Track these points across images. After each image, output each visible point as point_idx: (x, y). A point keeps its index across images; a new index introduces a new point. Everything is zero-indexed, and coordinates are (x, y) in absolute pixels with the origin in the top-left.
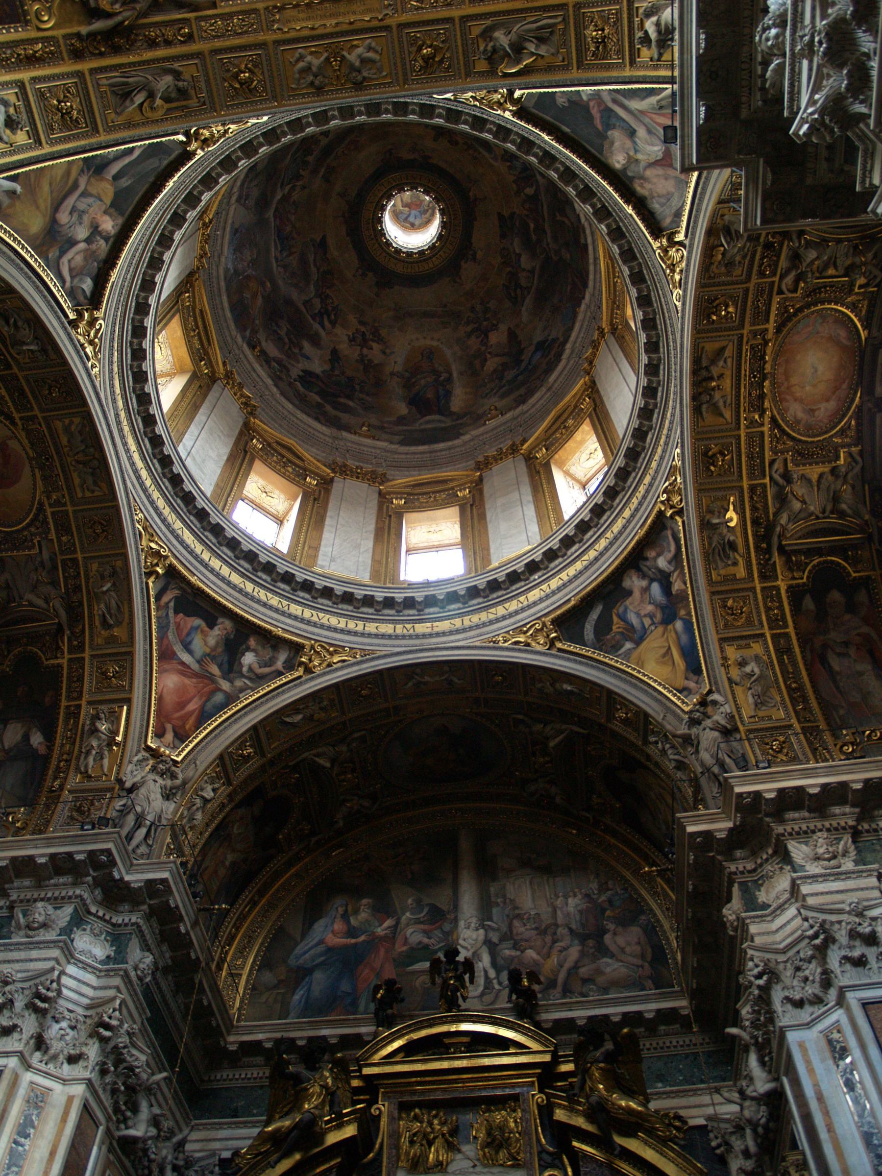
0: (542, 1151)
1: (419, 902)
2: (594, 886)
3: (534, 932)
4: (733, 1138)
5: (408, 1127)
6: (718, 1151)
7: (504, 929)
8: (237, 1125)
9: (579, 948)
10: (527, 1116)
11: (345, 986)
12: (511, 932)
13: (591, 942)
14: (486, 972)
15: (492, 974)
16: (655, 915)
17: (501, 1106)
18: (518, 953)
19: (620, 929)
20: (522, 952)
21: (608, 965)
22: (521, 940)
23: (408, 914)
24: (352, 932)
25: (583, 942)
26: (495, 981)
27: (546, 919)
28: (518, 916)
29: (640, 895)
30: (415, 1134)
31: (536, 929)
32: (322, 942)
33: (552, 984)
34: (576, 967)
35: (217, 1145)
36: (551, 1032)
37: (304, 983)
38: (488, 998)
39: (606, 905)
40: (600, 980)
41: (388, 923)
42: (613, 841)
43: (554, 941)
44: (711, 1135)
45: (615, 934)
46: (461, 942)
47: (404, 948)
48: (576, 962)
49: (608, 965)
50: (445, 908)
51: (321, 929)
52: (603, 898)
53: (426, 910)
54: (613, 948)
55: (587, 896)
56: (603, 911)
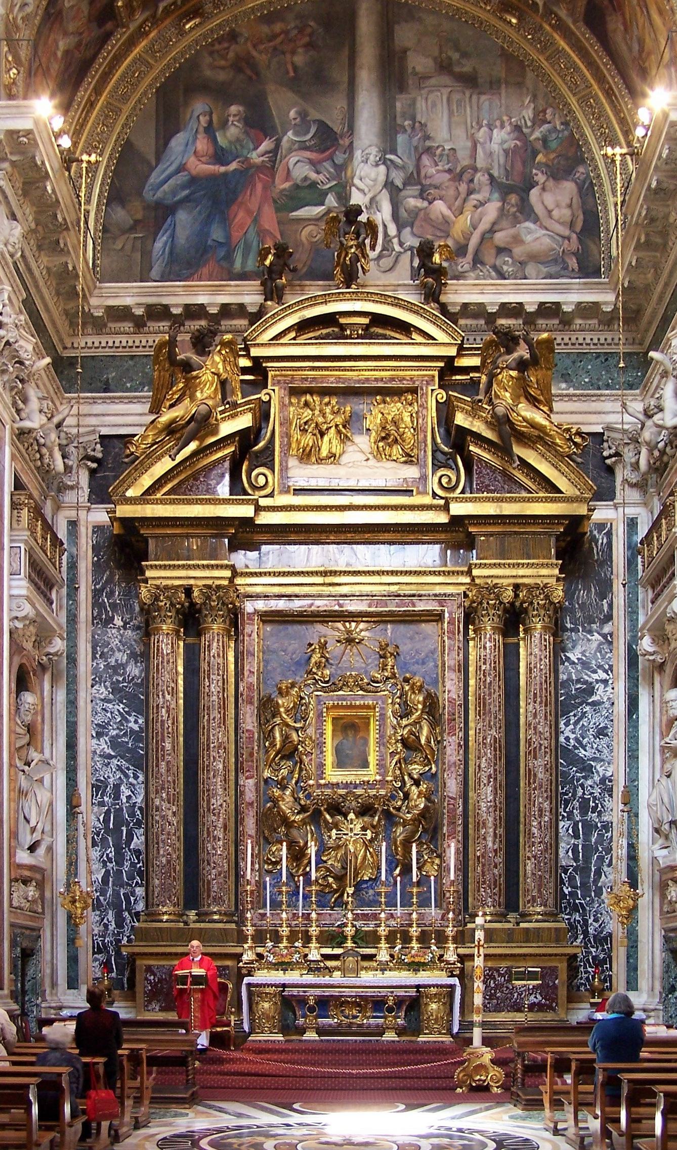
0: (436, 450)
1: (303, 115)
2: (528, 113)
3: (447, 176)
4: (626, 450)
5: (298, 413)
6: (608, 461)
7: (411, 168)
8: (113, 400)
9: (499, 204)
10: (424, 412)
11: (217, 234)
12: (419, 173)
13: (513, 199)
14: (385, 226)
15: (392, 230)
16: (596, 167)
17: (396, 398)
18: (426, 204)
19: (551, 183)
20: (430, 203)
21: (530, 232)
22: (430, 185)
23: (290, 134)
24: (220, 156)
25: (503, 200)
26: (395, 241)
27: (464, 160)
28: (429, 150)
29: (583, 135)
30: (306, 423)
31: (449, 171)
32: (182, 168)
33: (461, 250)
34: (492, 231)
35: (93, 421)
36: (453, 318)
37: (165, 226)
38: (386, 262)
39: (539, 145)
40: (518, 251)
41: (266, 145)
42: (563, 44)
43: (470, 192)
44: (605, 445)
45: (544, 189)
46: (356, 181)
47: (287, 185)
48: (494, 224)
49: (530, 232)
50: (337, 129)
51: (181, 148)
52: (537, 134)
53: (313, 130)
54: (539, 209)
55: (517, 128)
56: (535, 153)
